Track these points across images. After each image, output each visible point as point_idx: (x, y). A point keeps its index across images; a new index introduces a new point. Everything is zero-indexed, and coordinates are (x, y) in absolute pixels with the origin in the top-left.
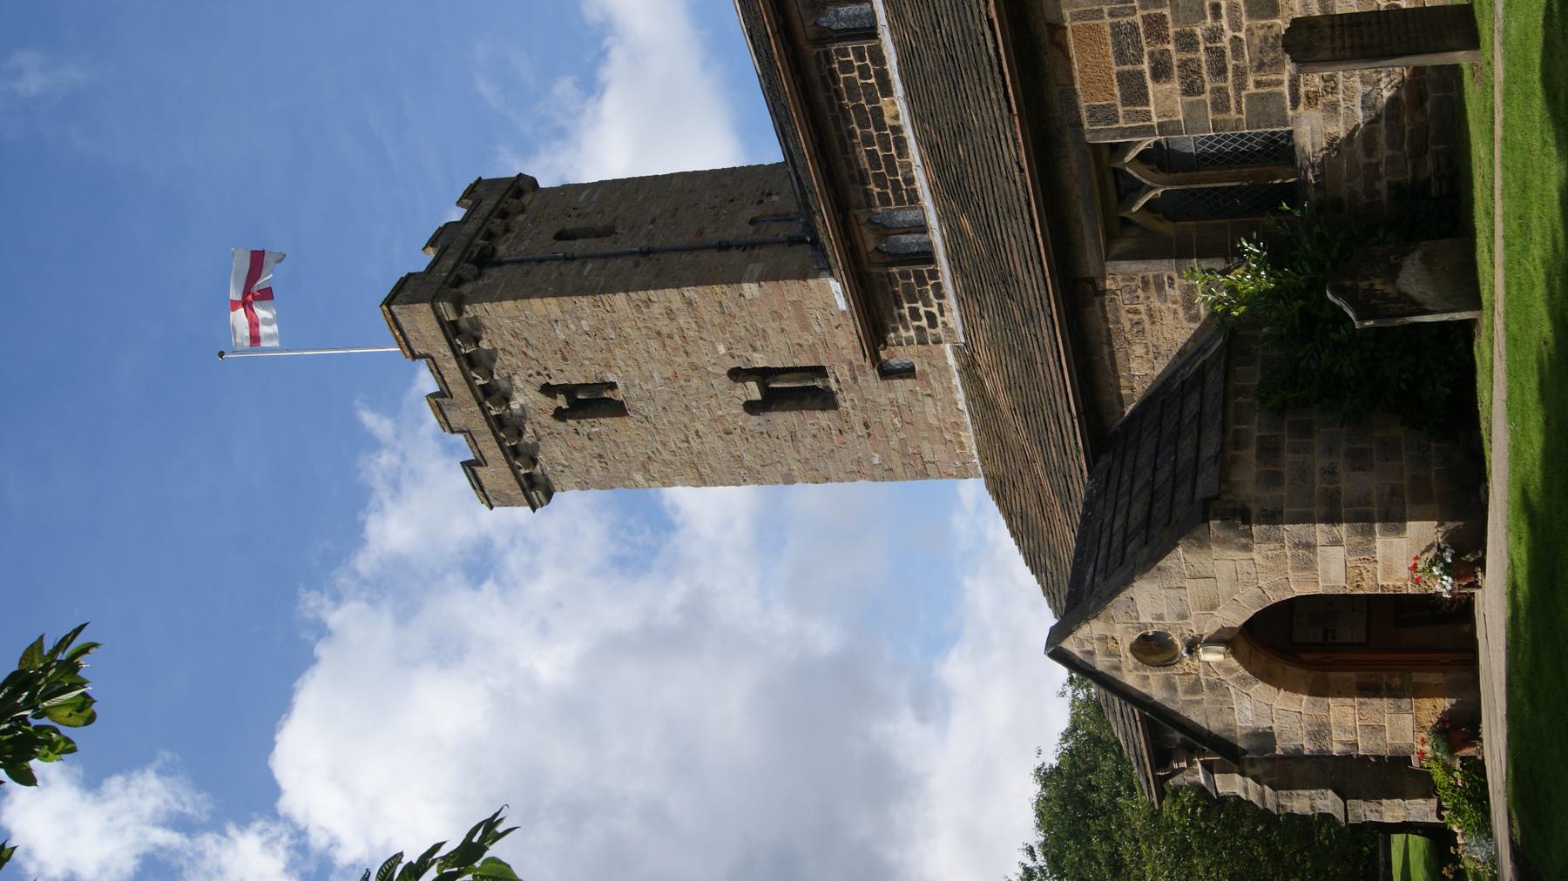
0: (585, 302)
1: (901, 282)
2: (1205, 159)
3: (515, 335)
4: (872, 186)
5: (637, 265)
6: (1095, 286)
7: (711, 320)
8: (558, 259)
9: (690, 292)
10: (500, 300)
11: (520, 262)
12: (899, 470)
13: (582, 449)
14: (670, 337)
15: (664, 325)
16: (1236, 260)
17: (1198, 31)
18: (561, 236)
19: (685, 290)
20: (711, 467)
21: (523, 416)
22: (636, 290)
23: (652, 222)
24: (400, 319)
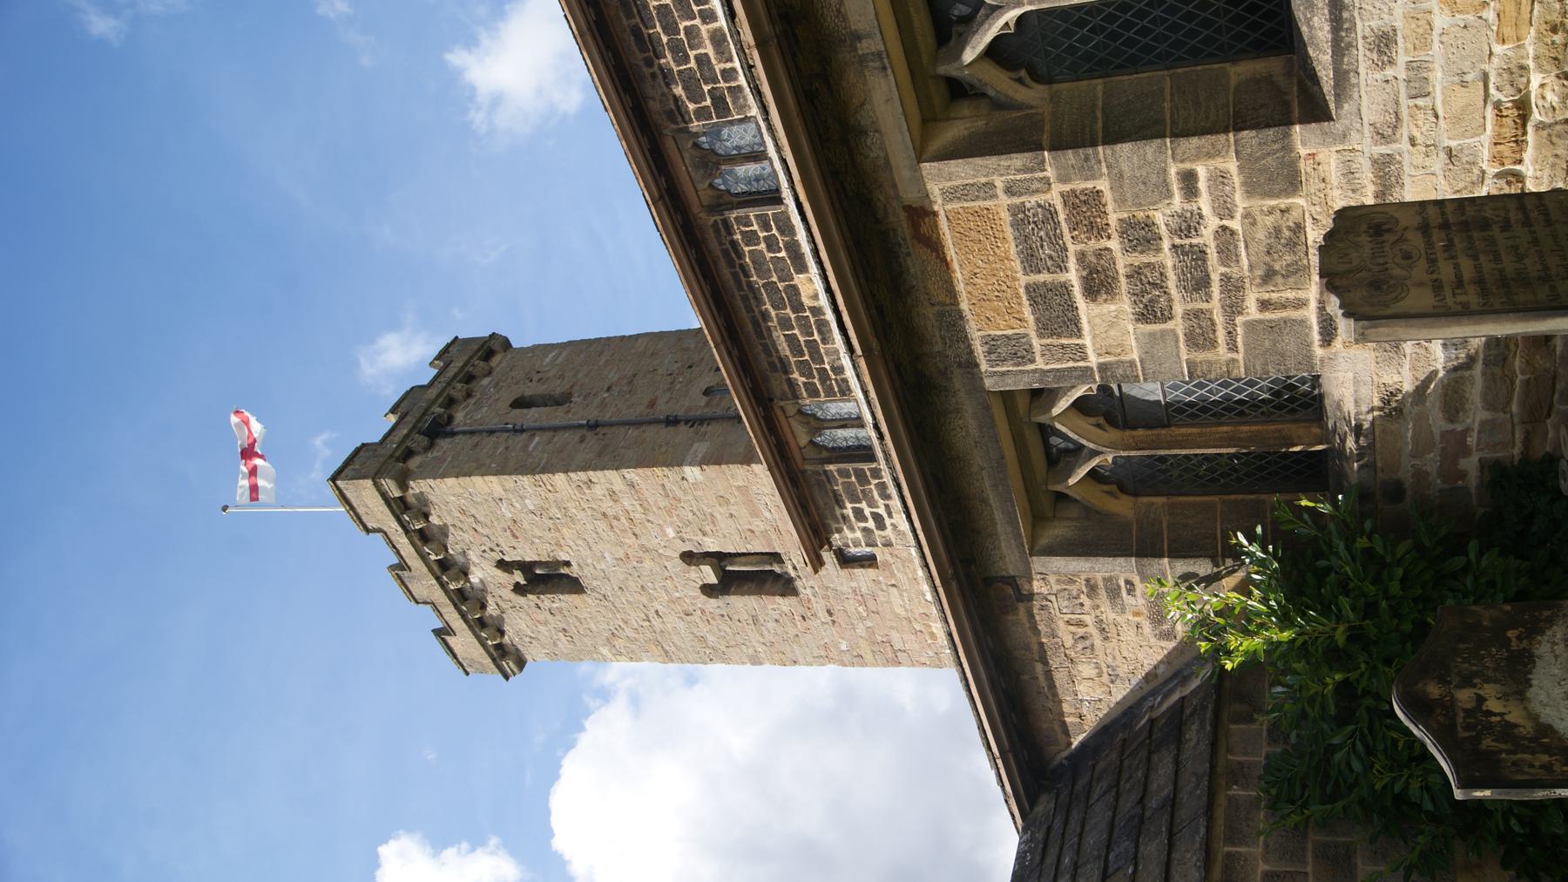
0: (526, 481)
1: (840, 480)
2: (1180, 411)
3: (463, 512)
4: (796, 375)
5: (582, 440)
6: (1017, 588)
7: (656, 501)
8: (507, 431)
9: (632, 474)
10: (443, 476)
11: (472, 433)
12: (868, 657)
13: (546, 623)
15: (607, 506)
16: (1229, 562)
17: (1159, 218)
18: (520, 403)
19: (625, 471)
20: (675, 646)
23: (609, 389)
24: (348, 494)
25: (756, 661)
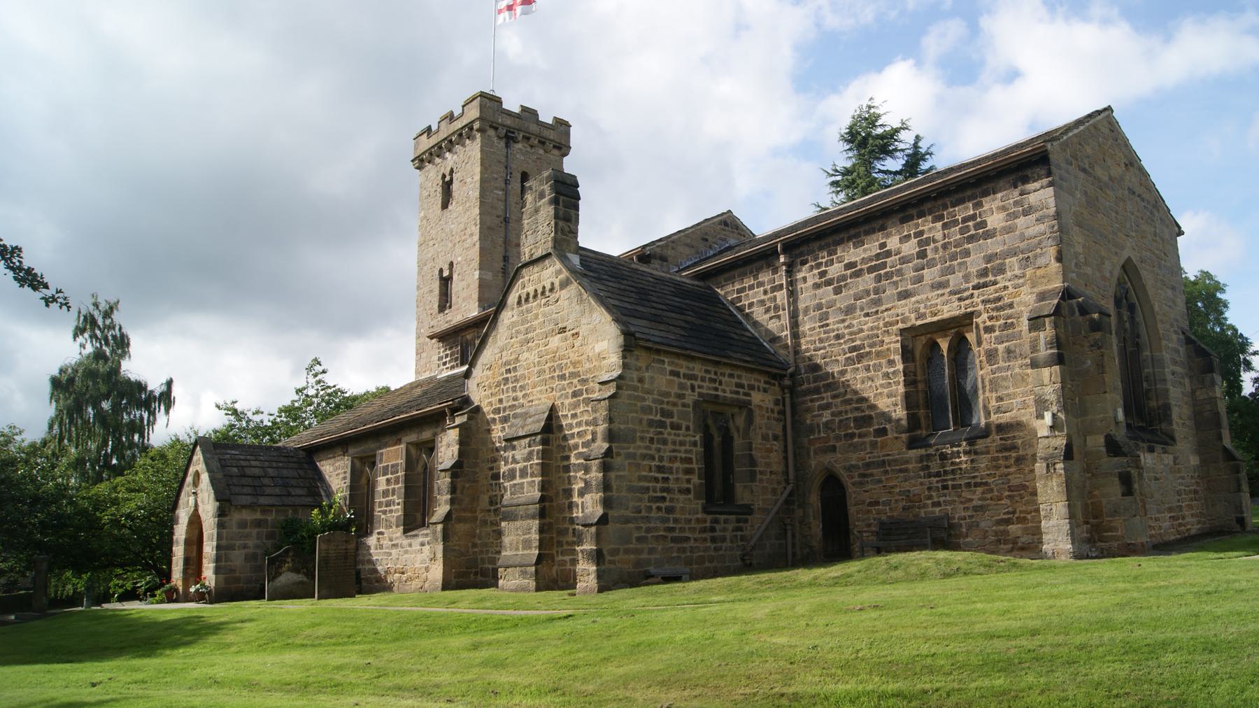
0: (477, 194)
14: (465, 234)
15: (468, 231)
21: (445, 159)
22: (481, 219)
25: (418, 288)
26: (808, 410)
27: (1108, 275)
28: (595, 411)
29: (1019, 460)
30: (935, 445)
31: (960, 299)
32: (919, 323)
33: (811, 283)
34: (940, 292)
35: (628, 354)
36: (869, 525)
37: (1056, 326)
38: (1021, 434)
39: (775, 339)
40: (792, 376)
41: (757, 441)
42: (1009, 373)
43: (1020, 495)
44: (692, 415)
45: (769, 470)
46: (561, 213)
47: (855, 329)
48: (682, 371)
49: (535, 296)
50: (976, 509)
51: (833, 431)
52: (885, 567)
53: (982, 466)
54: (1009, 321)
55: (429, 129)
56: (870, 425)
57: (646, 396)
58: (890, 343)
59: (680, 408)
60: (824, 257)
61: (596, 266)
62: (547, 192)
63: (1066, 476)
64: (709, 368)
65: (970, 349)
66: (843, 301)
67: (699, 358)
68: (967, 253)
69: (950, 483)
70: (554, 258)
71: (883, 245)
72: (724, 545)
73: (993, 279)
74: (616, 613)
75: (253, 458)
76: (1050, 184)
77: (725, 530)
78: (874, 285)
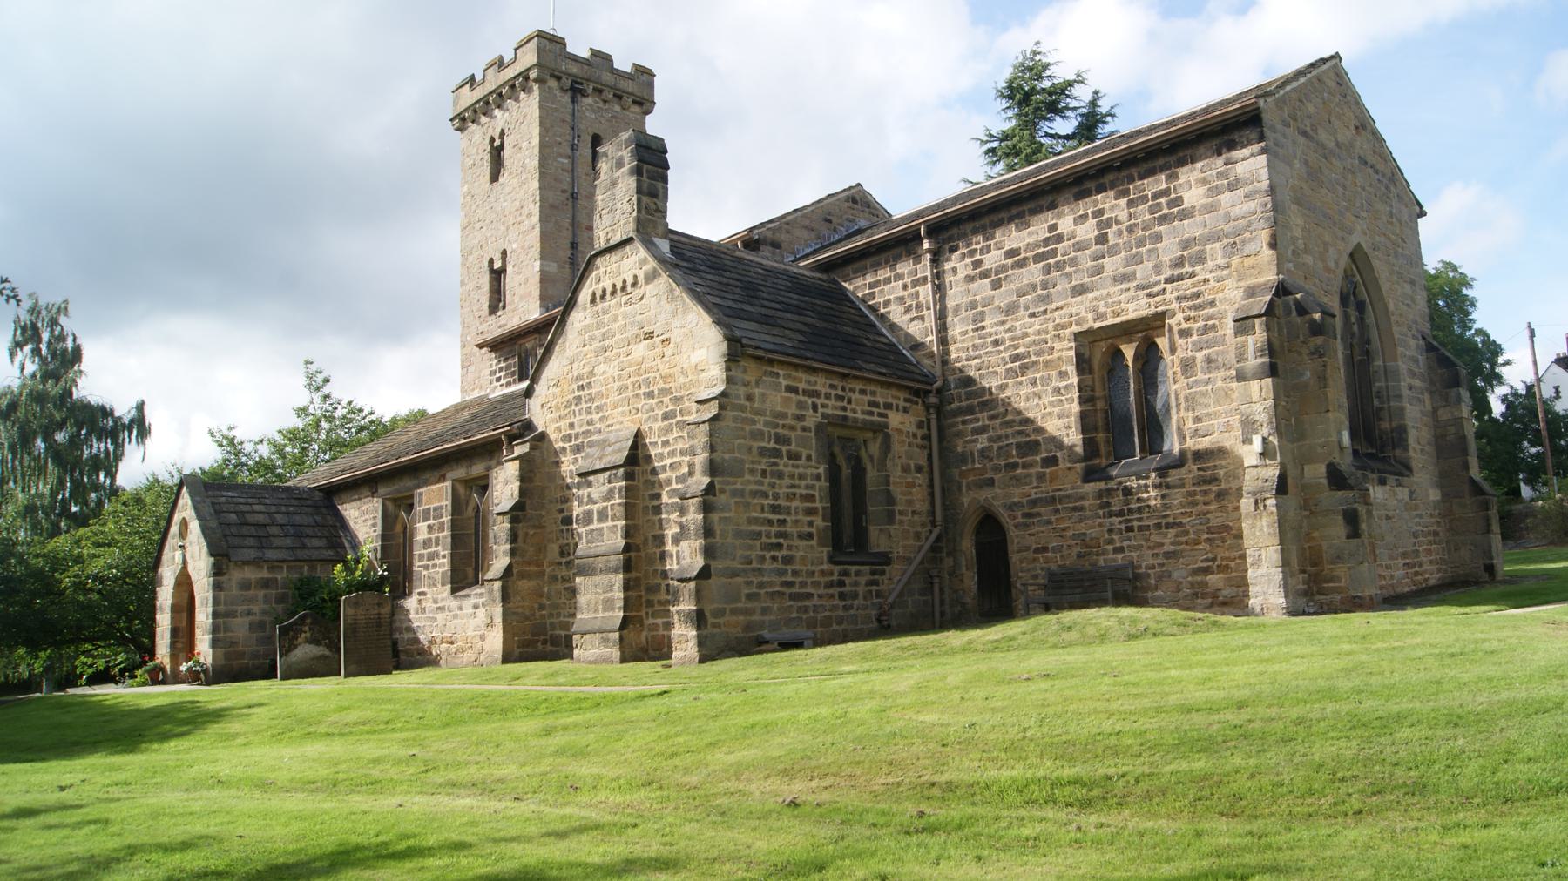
0: (536, 162)
15: (525, 211)
21: (493, 117)
25: (462, 283)
26: (960, 434)
27: (1332, 265)
28: (692, 437)
29: (1221, 495)
30: (1117, 476)
31: (1149, 296)
32: (1098, 325)
33: (963, 276)
34: (1124, 286)
35: (732, 365)
36: (1035, 577)
37: (1268, 329)
38: (1223, 463)
39: (917, 346)
40: (939, 391)
41: (896, 474)
42: (1210, 387)
43: (1222, 538)
44: (814, 442)
45: (910, 510)
46: (645, 186)
47: (1018, 333)
48: (802, 386)
49: (614, 293)
50: (1168, 555)
51: (991, 460)
52: (1056, 627)
53: (1176, 502)
54: (1210, 323)
55: (472, 79)
56: (1037, 452)
57: (756, 418)
58: (1062, 350)
59: (799, 432)
60: (978, 242)
61: (689, 254)
62: (627, 160)
63: (1279, 514)
64: (835, 383)
65: (1161, 358)
66: (1003, 297)
67: (822, 370)
68: (1158, 238)
69: (1136, 524)
70: (637, 244)
71: (1053, 228)
72: (856, 603)
73: (1190, 270)
74: (723, 687)
75: (255, 501)
76: (1263, 151)
77: (856, 584)
78: (1042, 277)
